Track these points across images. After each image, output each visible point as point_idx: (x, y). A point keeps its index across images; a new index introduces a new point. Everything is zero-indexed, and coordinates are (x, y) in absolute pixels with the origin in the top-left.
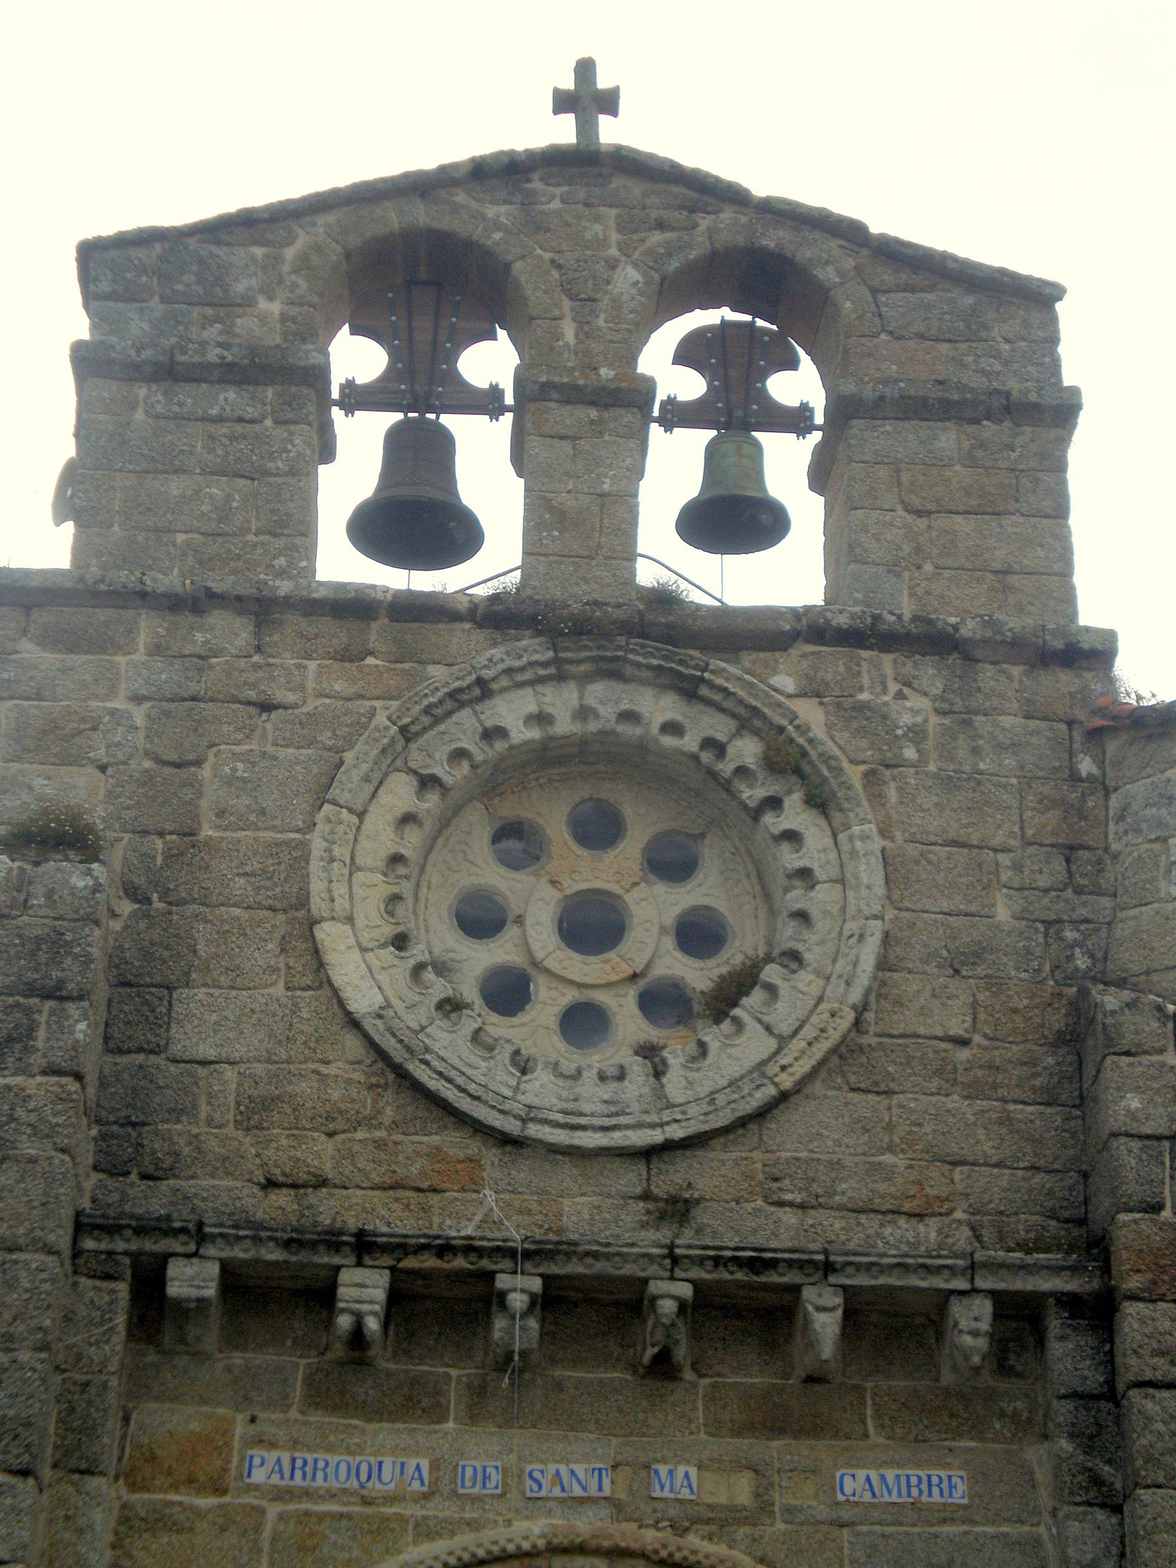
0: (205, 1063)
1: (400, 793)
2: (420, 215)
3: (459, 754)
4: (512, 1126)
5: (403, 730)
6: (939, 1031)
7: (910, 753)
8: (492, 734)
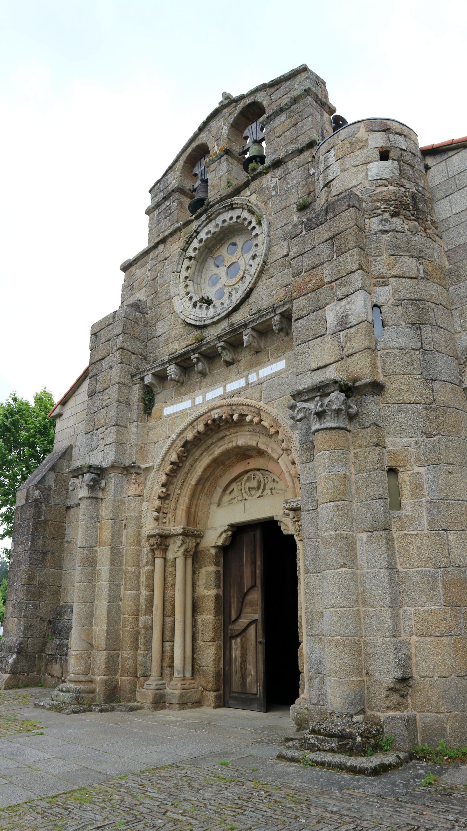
0: (160, 336)
1: (186, 263)
2: (194, 145)
3: (195, 249)
4: (202, 323)
5: (183, 250)
6: (281, 256)
7: (274, 193)
8: (201, 241)
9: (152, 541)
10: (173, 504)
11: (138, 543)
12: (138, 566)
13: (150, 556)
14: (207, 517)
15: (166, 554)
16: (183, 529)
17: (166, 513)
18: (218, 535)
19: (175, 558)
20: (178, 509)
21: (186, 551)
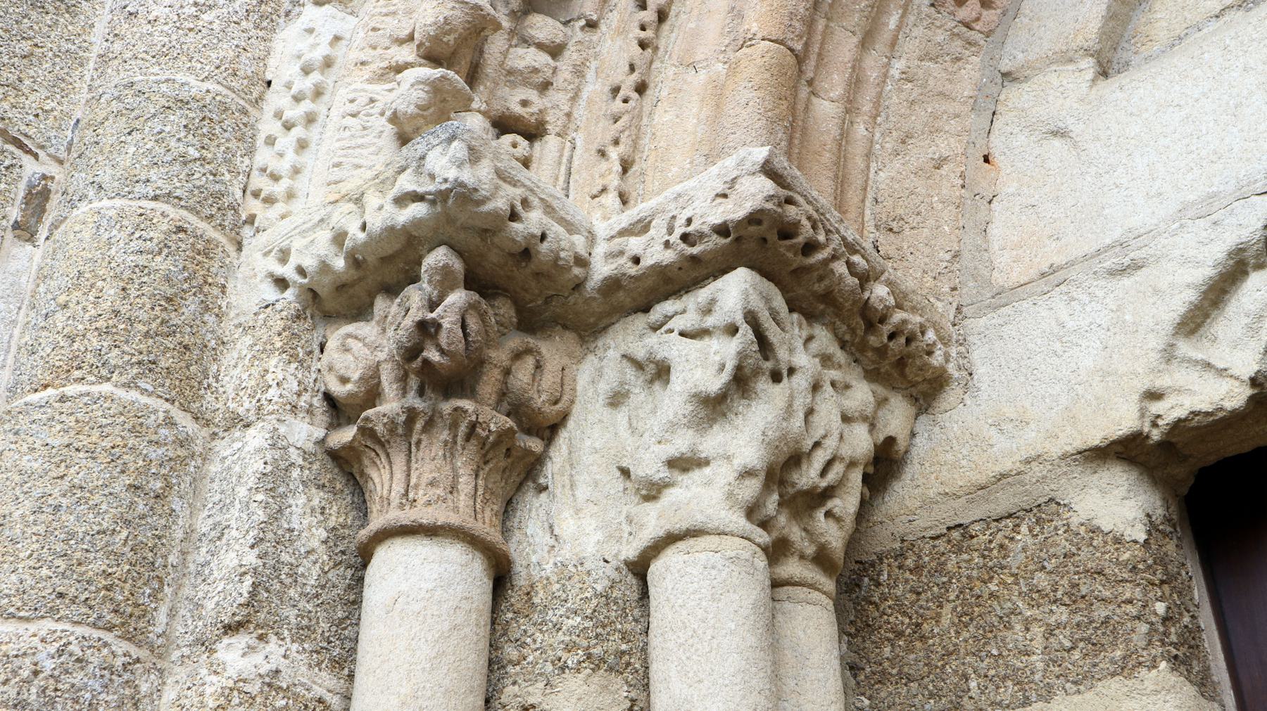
9: (360, 349)
10: (614, 48)
11: (171, 341)
12: (131, 622)
13: (310, 517)
14: (976, 200)
15: (508, 508)
16: (768, 170)
17: (533, 133)
18: (1182, 300)
19: (639, 568)
20: (661, 88)
21: (781, 469)
